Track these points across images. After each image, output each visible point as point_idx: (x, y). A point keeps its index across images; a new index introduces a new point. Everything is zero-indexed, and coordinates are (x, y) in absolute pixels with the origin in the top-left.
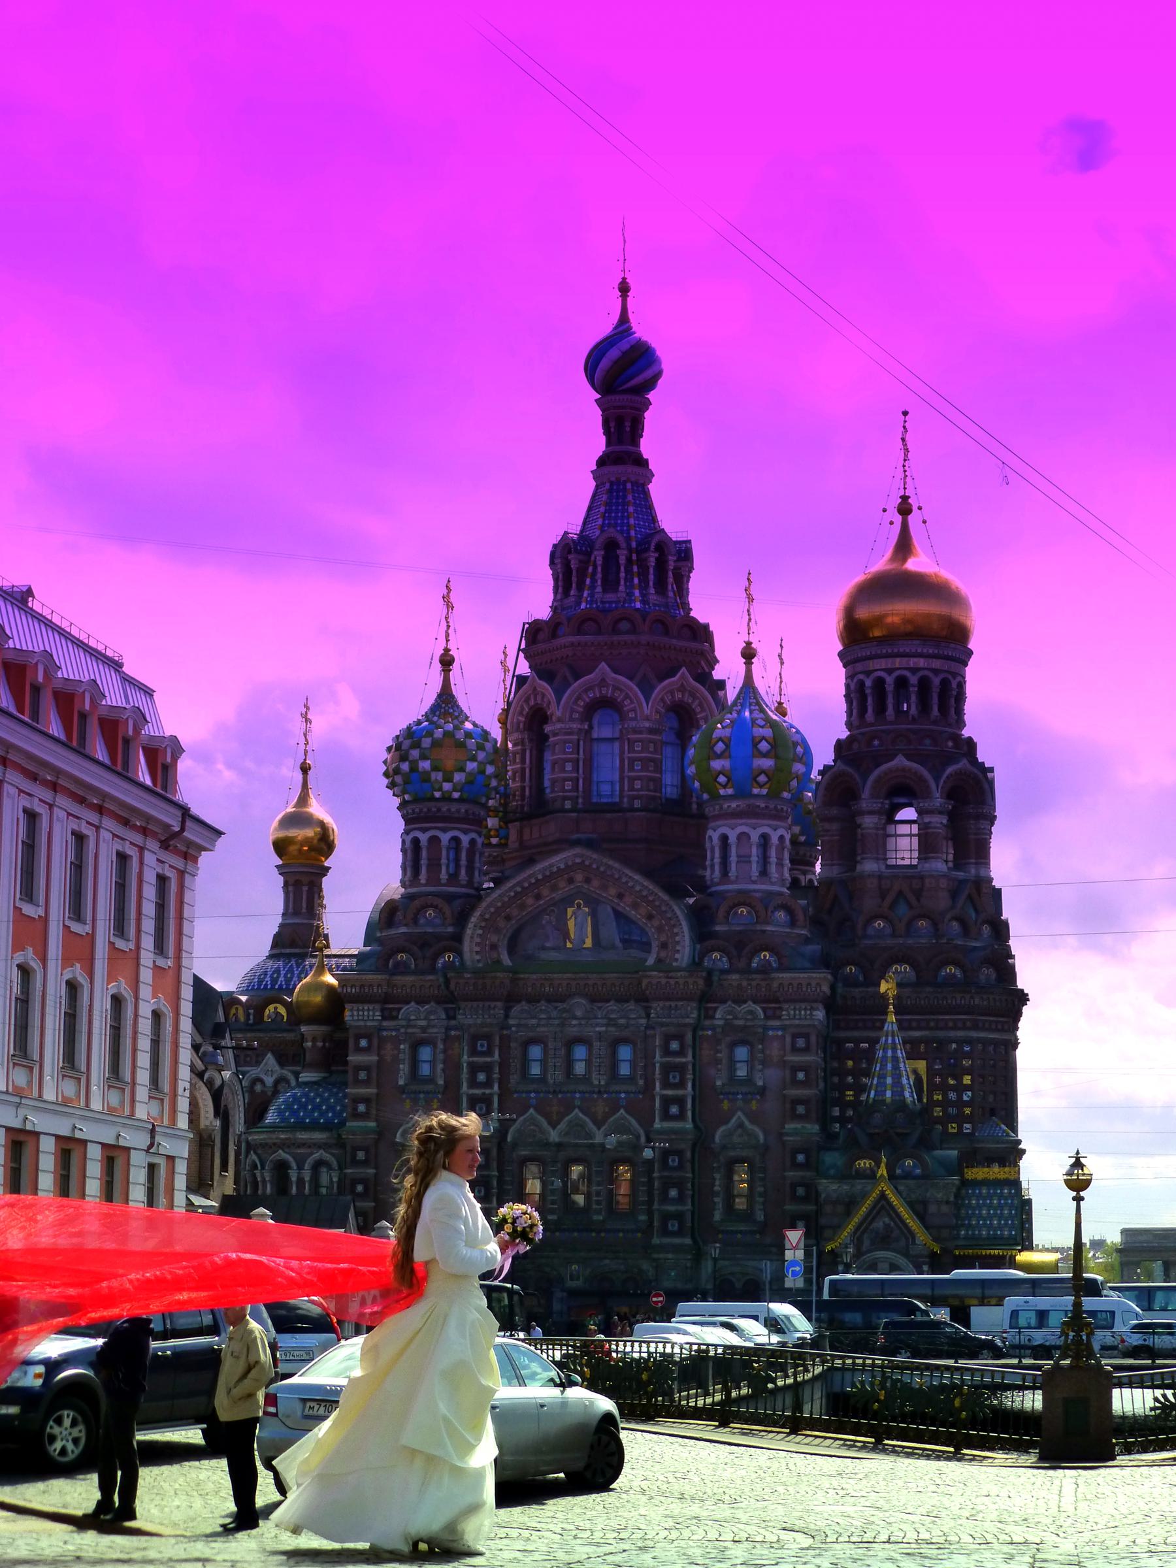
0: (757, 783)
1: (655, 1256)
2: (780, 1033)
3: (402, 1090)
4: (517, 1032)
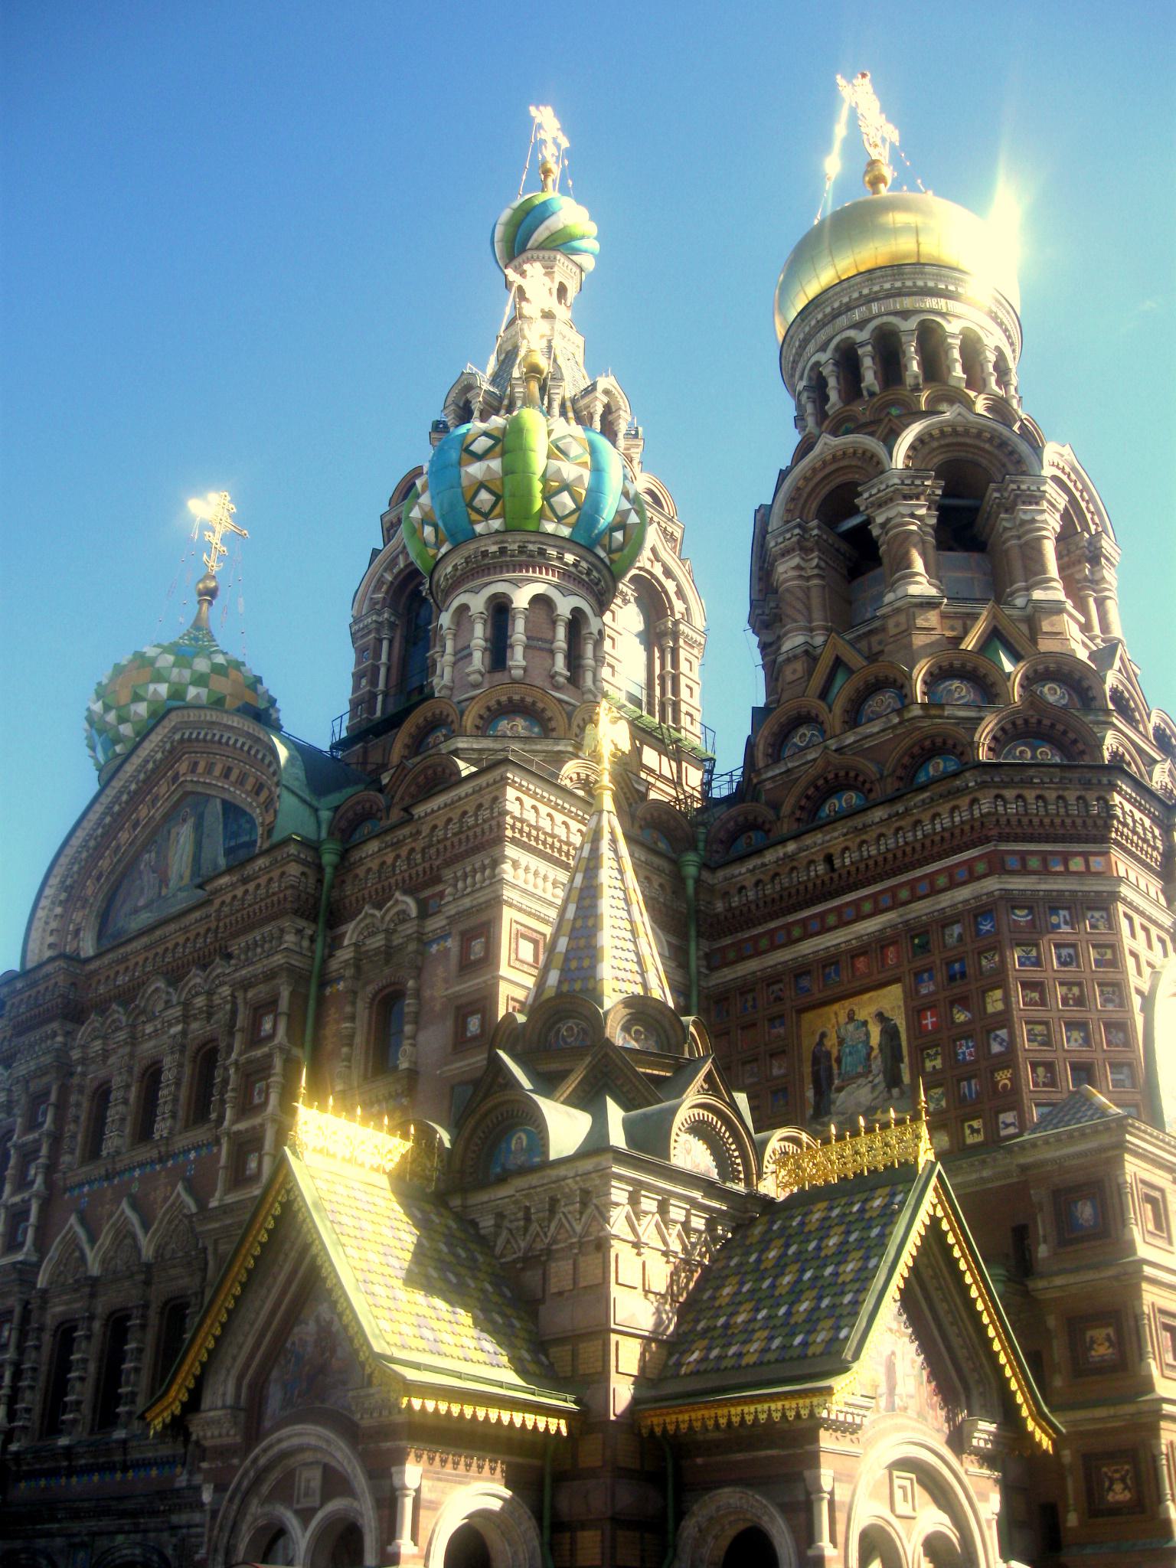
0: (478, 511)
1: (175, 1519)
4: (84, 1074)
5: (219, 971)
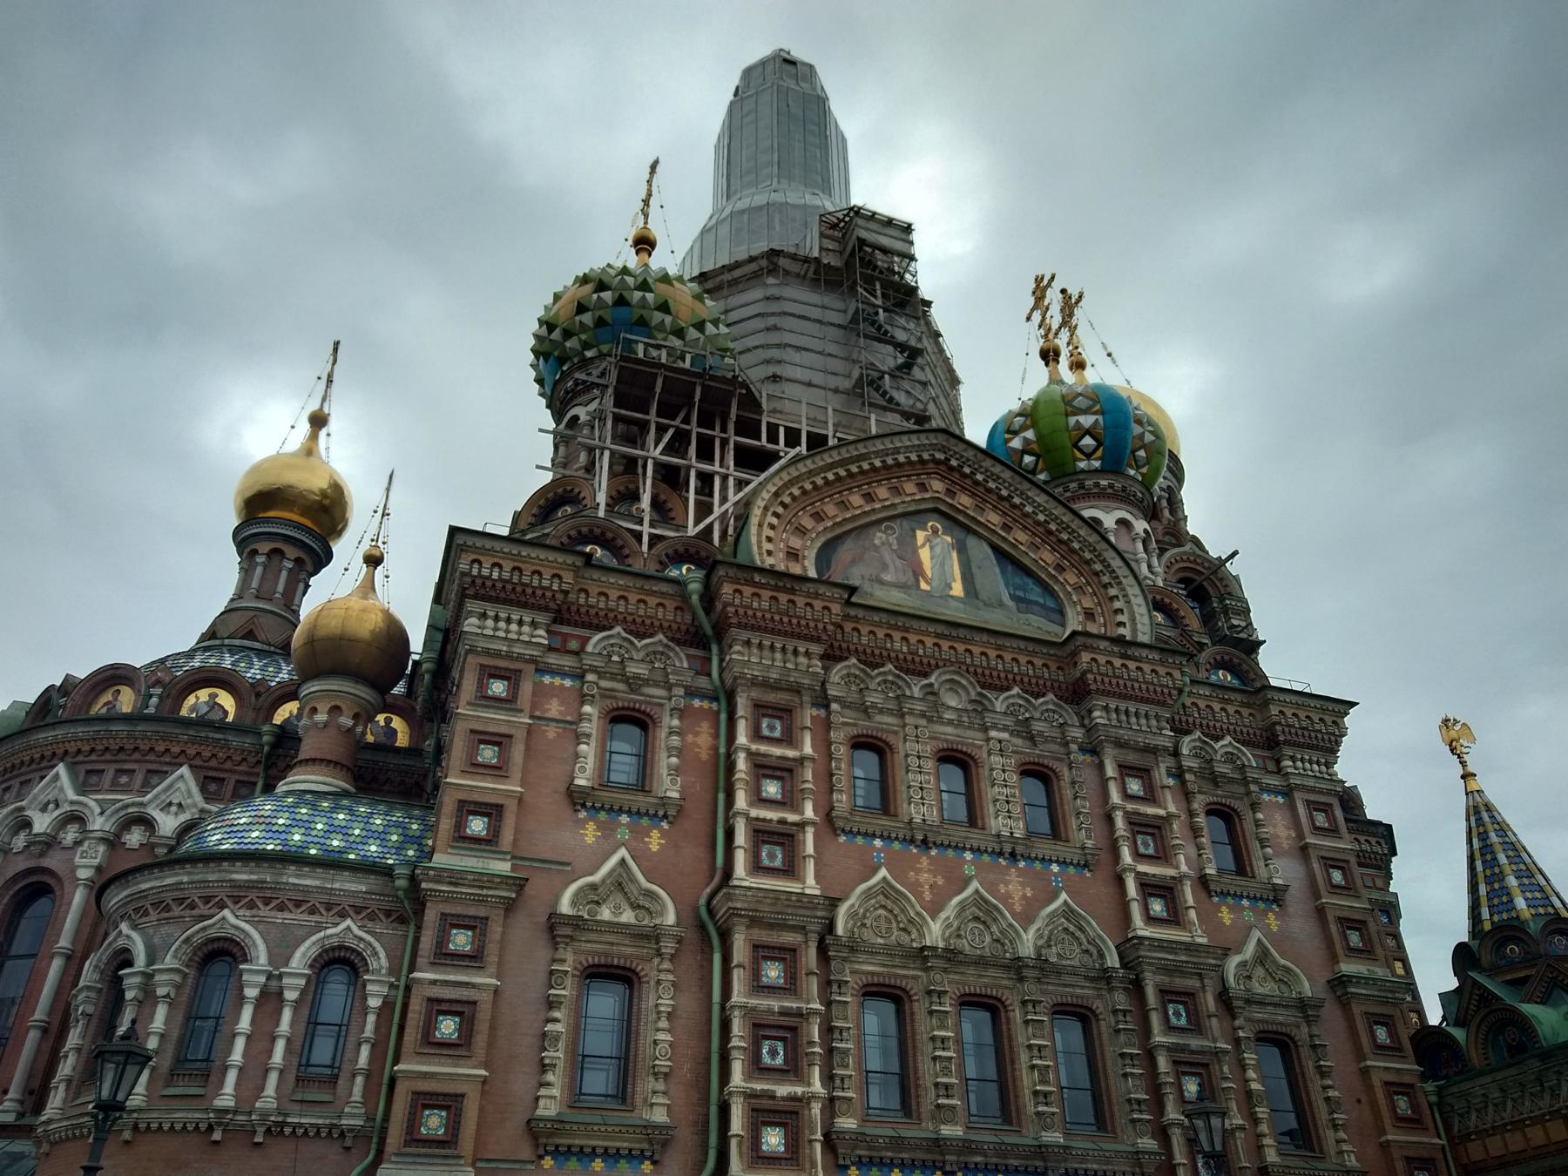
2: (1280, 799)
3: (577, 799)
5: (1051, 707)
